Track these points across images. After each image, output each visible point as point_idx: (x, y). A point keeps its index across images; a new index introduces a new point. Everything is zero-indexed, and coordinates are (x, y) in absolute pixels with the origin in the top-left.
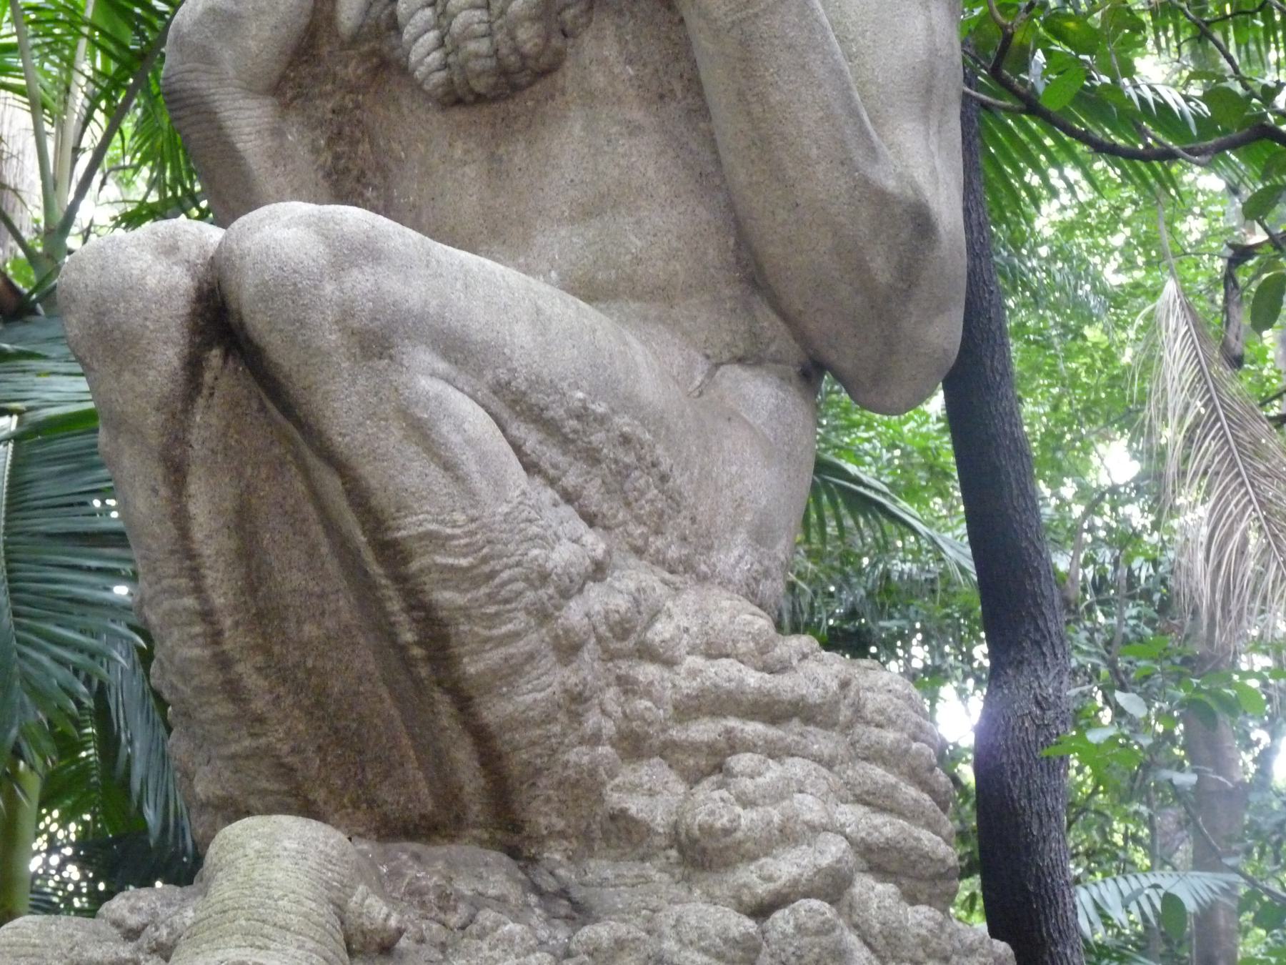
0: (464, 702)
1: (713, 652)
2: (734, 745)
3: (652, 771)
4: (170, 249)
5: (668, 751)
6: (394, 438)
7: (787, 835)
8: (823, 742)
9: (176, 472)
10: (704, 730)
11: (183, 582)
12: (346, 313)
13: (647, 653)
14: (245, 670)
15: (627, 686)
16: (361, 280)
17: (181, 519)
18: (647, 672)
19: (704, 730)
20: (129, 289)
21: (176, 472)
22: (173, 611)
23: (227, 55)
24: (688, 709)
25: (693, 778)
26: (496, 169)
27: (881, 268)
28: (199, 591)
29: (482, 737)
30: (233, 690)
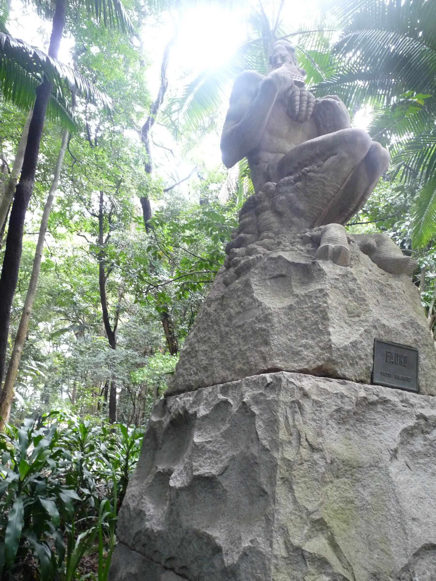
11: (341, 183)
22: (335, 186)
28: (341, 186)
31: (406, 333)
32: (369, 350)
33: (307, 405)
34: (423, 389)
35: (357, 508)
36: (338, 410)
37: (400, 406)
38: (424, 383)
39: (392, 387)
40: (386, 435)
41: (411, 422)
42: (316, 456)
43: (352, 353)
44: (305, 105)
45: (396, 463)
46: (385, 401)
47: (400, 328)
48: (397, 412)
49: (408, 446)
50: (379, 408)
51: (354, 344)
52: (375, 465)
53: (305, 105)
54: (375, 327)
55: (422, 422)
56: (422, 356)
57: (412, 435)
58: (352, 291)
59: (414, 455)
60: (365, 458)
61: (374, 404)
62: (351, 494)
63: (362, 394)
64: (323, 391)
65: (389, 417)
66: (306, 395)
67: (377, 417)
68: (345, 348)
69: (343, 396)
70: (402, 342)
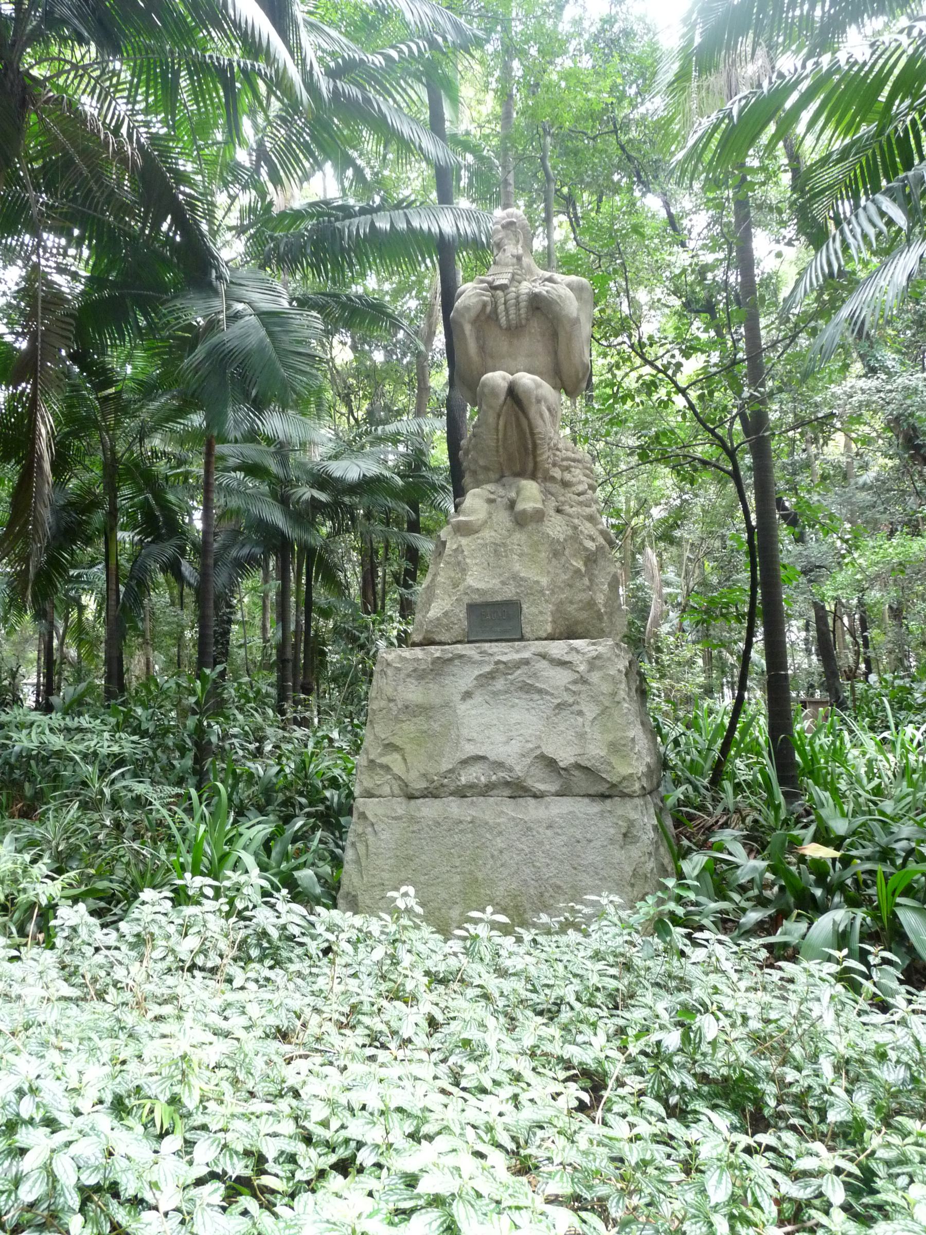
0: (535, 457)
1: (567, 450)
2: (570, 466)
3: (557, 469)
4: (504, 379)
5: (560, 466)
6: (538, 417)
7: (580, 482)
8: (580, 466)
9: (499, 416)
10: (565, 463)
12: (537, 397)
13: (558, 449)
14: (501, 450)
15: (555, 455)
16: (540, 391)
17: (498, 424)
18: (558, 453)
19: (565, 463)
20: (499, 386)
21: (499, 416)
23: (467, 316)
24: (563, 460)
25: (562, 471)
26: (511, 344)
27: (581, 376)
29: (536, 463)
30: (497, 451)
31: (505, 588)
32: (463, 615)
33: (390, 672)
34: (528, 635)
35: (429, 736)
36: (415, 670)
37: (477, 657)
38: (528, 630)
39: (491, 641)
40: (461, 682)
41: (487, 669)
42: (391, 705)
43: (445, 621)
44: (512, 311)
45: (470, 702)
46: (461, 657)
47: (500, 586)
48: (474, 663)
49: (490, 688)
50: (457, 662)
51: (446, 614)
52: (446, 705)
53: (512, 311)
54: (466, 594)
55: (501, 666)
56: (524, 606)
57: (493, 678)
58: (459, 563)
59: (495, 694)
60: (438, 701)
61: (450, 660)
62: (425, 727)
63: (438, 654)
64: (403, 659)
65: (466, 668)
66: (388, 664)
67: (456, 670)
68: (438, 619)
69: (419, 660)
70: (499, 599)
